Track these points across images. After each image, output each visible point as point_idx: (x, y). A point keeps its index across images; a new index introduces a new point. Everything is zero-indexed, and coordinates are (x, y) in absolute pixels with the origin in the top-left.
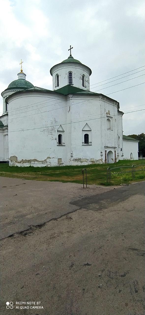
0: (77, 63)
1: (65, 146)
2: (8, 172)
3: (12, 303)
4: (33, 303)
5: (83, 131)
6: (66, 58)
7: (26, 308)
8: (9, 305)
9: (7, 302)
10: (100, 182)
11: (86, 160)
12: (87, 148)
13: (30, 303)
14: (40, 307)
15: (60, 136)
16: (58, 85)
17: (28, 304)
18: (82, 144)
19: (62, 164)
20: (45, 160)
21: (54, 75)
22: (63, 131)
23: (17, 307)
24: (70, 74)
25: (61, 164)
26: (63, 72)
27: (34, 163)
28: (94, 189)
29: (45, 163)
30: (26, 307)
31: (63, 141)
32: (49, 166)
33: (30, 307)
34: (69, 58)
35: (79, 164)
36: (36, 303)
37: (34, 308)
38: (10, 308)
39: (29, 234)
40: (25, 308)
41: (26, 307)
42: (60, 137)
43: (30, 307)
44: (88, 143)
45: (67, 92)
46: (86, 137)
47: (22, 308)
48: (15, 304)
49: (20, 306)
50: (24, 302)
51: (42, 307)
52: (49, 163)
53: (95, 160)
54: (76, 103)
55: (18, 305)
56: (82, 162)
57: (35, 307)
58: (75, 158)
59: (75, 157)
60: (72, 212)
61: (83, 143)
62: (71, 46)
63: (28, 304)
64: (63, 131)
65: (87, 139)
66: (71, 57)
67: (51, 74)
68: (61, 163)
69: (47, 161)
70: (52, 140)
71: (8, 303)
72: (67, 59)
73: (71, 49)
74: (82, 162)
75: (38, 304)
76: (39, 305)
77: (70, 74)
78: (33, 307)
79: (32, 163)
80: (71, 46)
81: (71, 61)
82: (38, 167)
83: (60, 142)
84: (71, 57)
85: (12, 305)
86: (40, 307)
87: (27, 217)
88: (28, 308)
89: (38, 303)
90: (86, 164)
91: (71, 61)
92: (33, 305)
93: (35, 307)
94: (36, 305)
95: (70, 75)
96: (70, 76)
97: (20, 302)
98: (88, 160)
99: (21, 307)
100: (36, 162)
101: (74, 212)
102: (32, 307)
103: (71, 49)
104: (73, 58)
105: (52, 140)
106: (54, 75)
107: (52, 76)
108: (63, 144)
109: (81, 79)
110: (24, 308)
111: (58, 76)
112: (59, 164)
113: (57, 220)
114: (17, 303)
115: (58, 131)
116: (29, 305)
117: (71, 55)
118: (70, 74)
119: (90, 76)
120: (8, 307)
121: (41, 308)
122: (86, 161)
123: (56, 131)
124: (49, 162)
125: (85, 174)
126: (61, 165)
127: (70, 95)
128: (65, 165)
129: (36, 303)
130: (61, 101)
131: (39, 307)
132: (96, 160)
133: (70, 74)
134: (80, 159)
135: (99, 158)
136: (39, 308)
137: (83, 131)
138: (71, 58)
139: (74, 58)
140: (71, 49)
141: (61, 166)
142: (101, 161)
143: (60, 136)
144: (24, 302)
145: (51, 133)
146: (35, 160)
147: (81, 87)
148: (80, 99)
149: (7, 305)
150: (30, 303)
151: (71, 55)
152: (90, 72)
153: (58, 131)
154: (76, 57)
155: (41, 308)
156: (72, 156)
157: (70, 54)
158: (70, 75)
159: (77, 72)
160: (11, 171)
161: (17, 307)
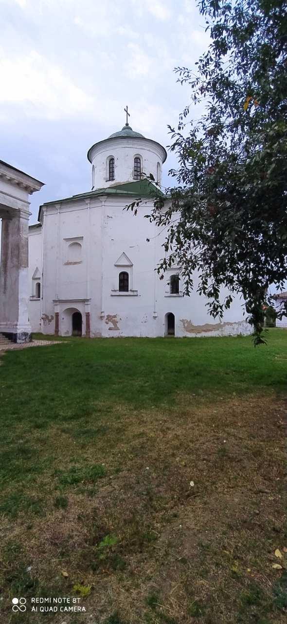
4: (66, 600)
6: (117, 127)
7: (51, 611)
8: (19, 604)
13: (60, 601)
17: (56, 602)
30: (51, 607)
33: (59, 609)
34: (124, 129)
36: (71, 601)
41: (51, 607)
43: (59, 609)
47: (43, 611)
48: (30, 605)
50: (48, 599)
55: (36, 605)
57: (69, 608)
63: (56, 602)
67: (89, 160)
75: (74, 601)
76: (77, 604)
78: (66, 608)
81: (127, 136)
86: (79, 608)
92: (65, 604)
93: (69, 608)
99: (42, 609)
102: (63, 609)
104: (131, 129)
107: (91, 163)
116: (58, 605)
117: (127, 124)
119: (163, 163)
129: (71, 601)
131: (77, 608)
136: (77, 610)
138: (127, 130)
149: (14, 605)
151: (127, 124)
154: (137, 127)
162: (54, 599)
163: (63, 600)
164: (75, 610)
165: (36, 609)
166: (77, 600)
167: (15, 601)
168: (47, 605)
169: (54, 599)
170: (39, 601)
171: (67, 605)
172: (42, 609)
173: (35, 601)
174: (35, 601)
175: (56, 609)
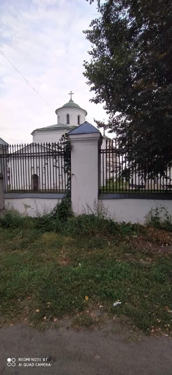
0: (77, 107)
3: (13, 360)
4: (39, 359)
6: (67, 101)
7: (30, 366)
8: (11, 362)
9: (8, 358)
13: (35, 359)
14: (47, 364)
17: (33, 360)
23: (20, 364)
30: (30, 364)
33: (35, 364)
34: (70, 101)
36: (42, 360)
38: (11, 363)
40: (29, 365)
41: (30, 364)
43: (35, 364)
47: (25, 366)
48: (17, 363)
49: (22, 362)
50: (28, 359)
66: (71, 101)
71: (9, 360)
72: (68, 102)
73: (71, 94)
75: (44, 360)
76: (45, 362)
80: (71, 91)
84: (71, 101)
85: (14, 362)
88: (33, 365)
89: (44, 360)
94: (42, 362)
97: (23, 359)
99: (25, 365)
102: (37, 365)
103: (71, 94)
110: (27, 365)
114: (19, 359)
116: (34, 362)
117: (71, 99)
120: (9, 364)
121: (48, 365)
129: (42, 360)
131: (45, 364)
139: (75, 102)
150: (35, 359)
151: (71, 99)
152: (86, 114)
154: (76, 102)
155: (48, 365)
161: (20, 364)
162: (32, 359)
163: (37, 359)
165: (21, 365)
166: (45, 359)
167: (9, 360)
168: (27, 362)
169: (32, 359)
170: (23, 360)
174: (21, 360)
175: (33, 364)
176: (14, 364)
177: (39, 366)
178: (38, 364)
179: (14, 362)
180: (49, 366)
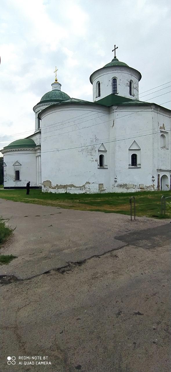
1: (108, 169)
2: (41, 199)
3: (14, 358)
4: (39, 357)
5: (130, 150)
6: (109, 60)
8: (11, 360)
10: (151, 213)
11: (133, 186)
12: (135, 171)
15: (101, 157)
16: (99, 95)
18: (128, 166)
19: (104, 190)
20: (84, 186)
21: (95, 82)
22: (105, 151)
24: (114, 81)
25: (102, 190)
26: (106, 80)
27: (71, 189)
28: (145, 222)
29: (83, 189)
30: (30, 362)
31: (105, 162)
32: (88, 193)
33: (35, 362)
35: (124, 191)
36: (42, 358)
37: (40, 363)
39: (67, 272)
40: (29, 363)
42: (101, 158)
43: (35, 362)
44: (136, 165)
45: (111, 103)
46: (134, 158)
47: (25, 364)
49: (23, 361)
50: (29, 357)
51: (50, 363)
52: (88, 189)
53: (144, 186)
54: (121, 115)
55: (21, 360)
56: (128, 188)
57: (41, 362)
58: (120, 184)
59: (120, 182)
60: (117, 249)
61: (129, 165)
62: (115, 46)
64: (105, 151)
65: (135, 161)
66: (115, 59)
68: (103, 189)
69: (86, 187)
70: (92, 162)
71: (9, 358)
72: (111, 61)
73: (115, 49)
74: (128, 188)
75: (44, 358)
76: (45, 360)
77: (115, 80)
78: (39, 362)
79: (68, 189)
80: (115, 46)
82: (76, 194)
83: (101, 164)
84: (115, 59)
85: (14, 361)
86: (47, 363)
87: (64, 251)
89: (44, 358)
90: (133, 191)
91: (116, 65)
92: (38, 360)
93: (41, 362)
95: (115, 82)
96: (114, 83)
98: (136, 186)
99: (25, 363)
100: (73, 188)
101: (120, 248)
102: (37, 363)
103: (115, 49)
104: (118, 60)
105: (92, 162)
106: (95, 82)
108: (105, 166)
109: (128, 86)
111: (99, 84)
112: (100, 190)
113: (100, 257)
115: (99, 151)
117: (115, 57)
118: (114, 81)
120: (9, 363)
121: (48, 363)
122: (134, 187)
123: (97, 151)
124: (88, 188)
125: (133, 204)
126: (102, 191)
127: (114, 106)
128: (107, 192)
129: (42, 358)
130: (102, 114)
131: (46, 362)
132: (145, 186)
133: (115, 80)
134: (126, 185)
135: (150, 183)
137: (130, 150)
138: (115, 61)
140: (114, 49)
141: (102, 193)
142: (152, 187)
143: (101, 157)
144: (29, 357)
145: (91, 153)
146: (72, 186)
147: (128, 96)
148: (126, 110)
149: (8, 360)
151: (115, 57)
153: (99, 151)
154: (121, 59)
155: (48, 363)
156: (116, 181)
157: (114, 56)
158: (115, 82)
159: (123, 77)
160: (44, 198)
162: (32, 357)
163: (37, 357)
164: (45, 364)
166: (46, 358)
167: (9, 358)
168: (27, 360)
170: (23, 358)
171: (41, 361)
172: (25, 363)
173: (21, 358)
174: (21, 358)
175: (33, 363)
176: (13, 363)
177: (39, 364)
178: (38, 362)
179: (14, 361)
180: (50, 364)
